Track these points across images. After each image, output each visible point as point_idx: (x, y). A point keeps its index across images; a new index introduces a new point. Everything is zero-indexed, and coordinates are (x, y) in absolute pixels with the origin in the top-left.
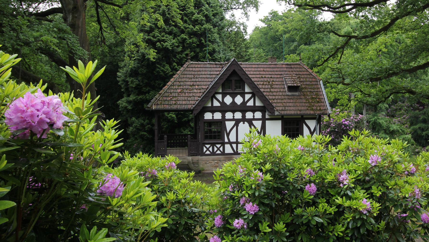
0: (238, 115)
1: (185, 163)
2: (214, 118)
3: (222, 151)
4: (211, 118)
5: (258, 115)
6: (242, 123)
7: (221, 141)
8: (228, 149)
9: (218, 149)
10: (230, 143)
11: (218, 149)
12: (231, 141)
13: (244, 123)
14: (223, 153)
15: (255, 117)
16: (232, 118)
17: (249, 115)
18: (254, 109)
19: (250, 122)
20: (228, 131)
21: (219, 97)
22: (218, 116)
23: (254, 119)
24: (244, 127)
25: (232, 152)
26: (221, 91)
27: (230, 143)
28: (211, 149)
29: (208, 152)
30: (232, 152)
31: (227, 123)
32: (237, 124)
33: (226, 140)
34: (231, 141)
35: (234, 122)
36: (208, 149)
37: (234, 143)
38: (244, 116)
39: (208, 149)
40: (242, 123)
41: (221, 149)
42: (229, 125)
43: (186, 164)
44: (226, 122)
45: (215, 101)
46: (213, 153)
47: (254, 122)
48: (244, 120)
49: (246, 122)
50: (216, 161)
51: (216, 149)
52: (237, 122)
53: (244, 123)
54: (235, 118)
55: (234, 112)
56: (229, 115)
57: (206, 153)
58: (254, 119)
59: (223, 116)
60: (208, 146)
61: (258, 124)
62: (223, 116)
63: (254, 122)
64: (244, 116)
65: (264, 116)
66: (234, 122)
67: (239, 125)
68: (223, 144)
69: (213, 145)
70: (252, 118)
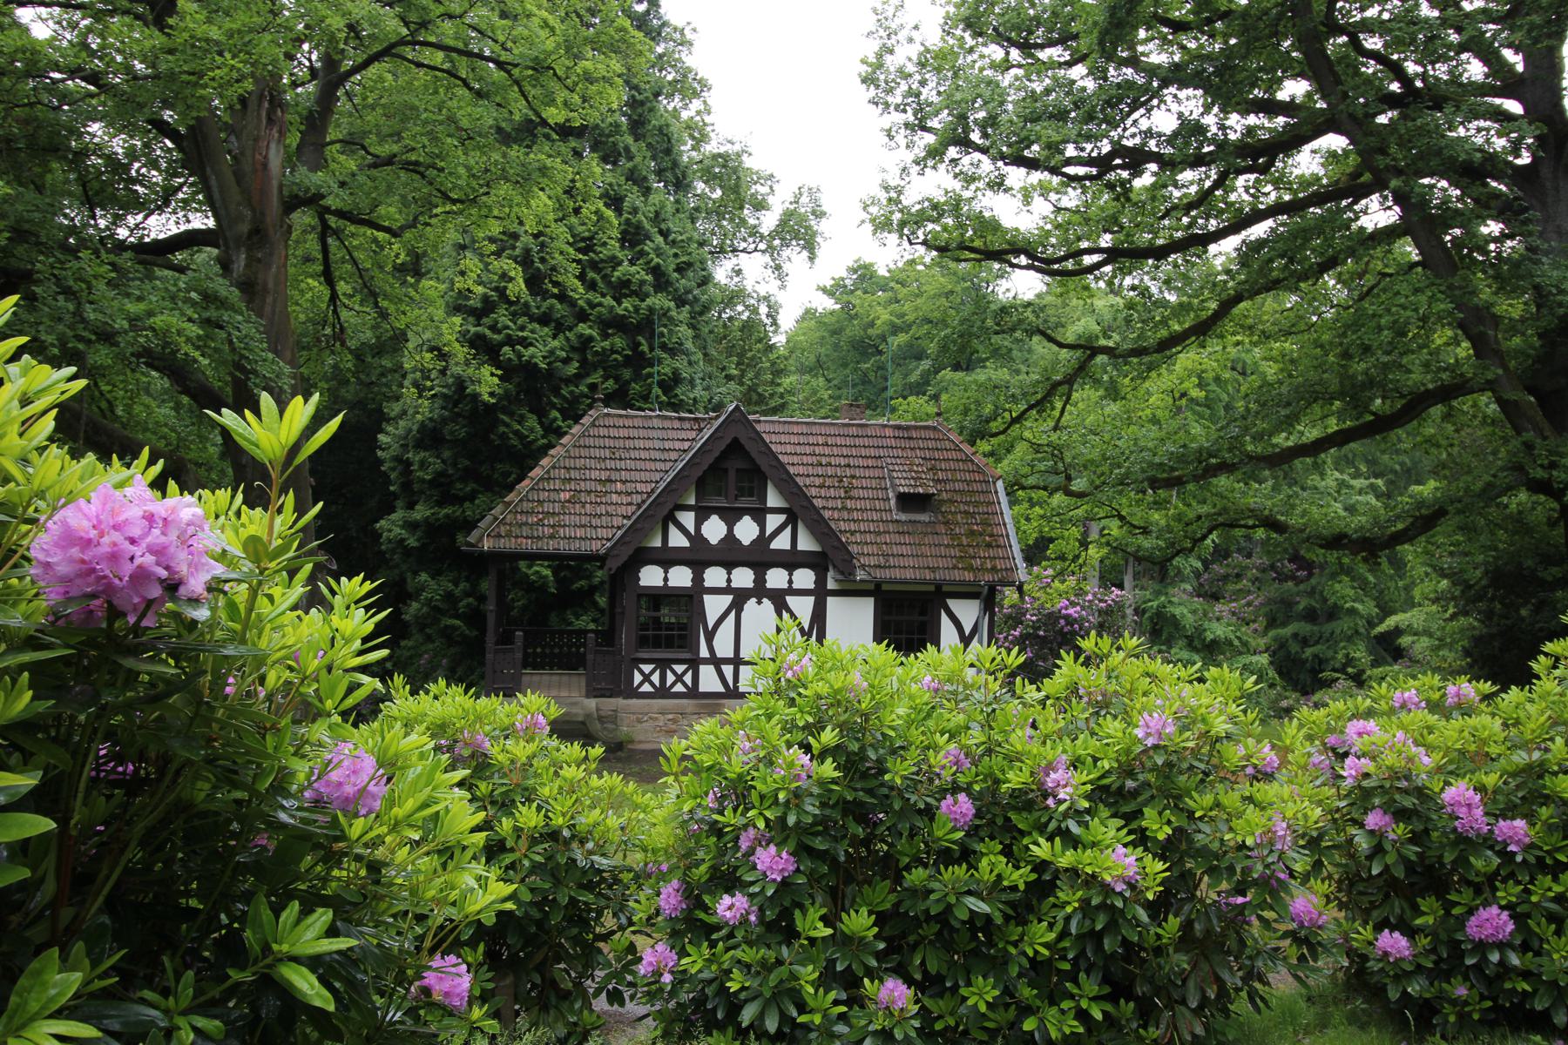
0: (743, 578)
2: (670, 584)
4: (661, 584)
5: (805, 578)
6: (754, 600)
7: (687, 656)
8: (709, 680)
9: (679, 678)
10: (717, 662)
11: (679, 678)
12: (719, 655)
13: (759, 603)
14: (693, 692)
15: (795, 586)
16: (724, 585)
17: (776, 578)
18: (791, 561)
19: (779, 600)
20: (710, 627)
21: (688, 519)
22: (681, 577)
23: (792, 591)
24: (759, 614)
25: (721, 689)
26: (692, 502)
27: (717, 662)
29: (646, 688)
30: (721, 689)
32: (737, 606)
33: (704, 652)
35: (728, 599)
36: (647, 678)
37: (727, 661)
38: (760, 580)
40: (754, 600)
41: (688, 678)
42: (714, 606)
44: (706, 598)
46: (663, 692)
47: (790, 600)
48: (759, 591)
49: (765, 600)
51: (670, 678)
52: (740, 598)
53: (759, 603)
54: (733, 585)
55: (729, 566)
56: (715, 576)
58: (792, 591)
59: (698, 579)
60: (647, 668)
61: (803, 607)
62: (698, 579)
63: (790, 600)
64: (760, 580)
65: (821, 581)
66: (727, 600)
68: (694, 663)
69: (663, 665)
70: (786, 586)
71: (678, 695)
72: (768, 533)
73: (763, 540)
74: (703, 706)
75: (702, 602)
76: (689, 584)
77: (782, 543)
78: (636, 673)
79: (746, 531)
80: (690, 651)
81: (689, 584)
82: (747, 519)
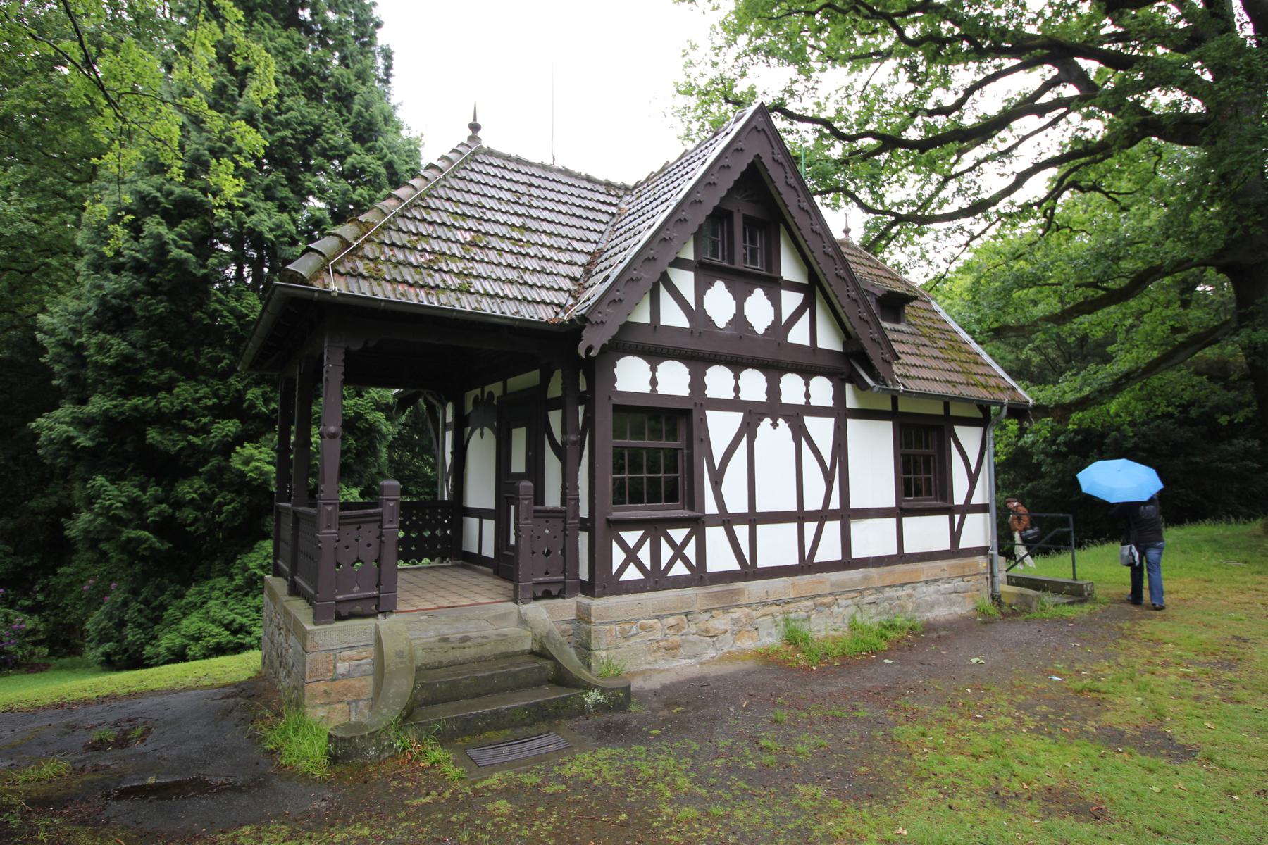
0: (754, 385)
1: (517, 648)
2: (661, 390)
3: (693, 561)
4: (647, 389)
6: (767, 421)
10: (727, 521)
12: (731, 510)
13: (775, 425)
14: (699, 576)
17: (792, 389)
19: (795, 417)
21: (685, 281)
25: (735, 566)
26: (689, 254)
27: (727, 521)
28: (645, 555)
29: (632, 573)
30: (735, 566)
31: (712, 416)
32: (748, 430)
33: (711, 507)
34: (731, 510)
35: (736, 418)
36: (631, 555)
37: (739, 518)
38: (773, 391)
39: (631, 555)
40: (767, 421)
41: (690, 551)
43: (523, 653)
44: (712, 416)
45: (665, 298)
46: (656, 579)
47: (811, 422)
48: (773, 408)
49: (781, 421)
50: (672, 621)
51: (667, 552)
52: (753, 415)
53: (775, 425)
54: (744, 396)
55: (737, 365)
56: (719, 381)
57: (624, 578)
59: (697, 384)
60: (631, 537)
62: (697, 384)
63: (811, 422)
64: (773, 391)
65: (839, 396)
66: (736, 418)
67: (759, 430)
68: (697, 525)
70: (802, 401)
71: (679, 582)
72: (785, 318)
73: (779, 328)
74: (717, 596)
75: (703, 421)
76: (685, 391)
77: (799, 335)
78: (615, 547)
79: (759, 311)
80: (692, 508)
81: (685, 391)
82: (759, 293)
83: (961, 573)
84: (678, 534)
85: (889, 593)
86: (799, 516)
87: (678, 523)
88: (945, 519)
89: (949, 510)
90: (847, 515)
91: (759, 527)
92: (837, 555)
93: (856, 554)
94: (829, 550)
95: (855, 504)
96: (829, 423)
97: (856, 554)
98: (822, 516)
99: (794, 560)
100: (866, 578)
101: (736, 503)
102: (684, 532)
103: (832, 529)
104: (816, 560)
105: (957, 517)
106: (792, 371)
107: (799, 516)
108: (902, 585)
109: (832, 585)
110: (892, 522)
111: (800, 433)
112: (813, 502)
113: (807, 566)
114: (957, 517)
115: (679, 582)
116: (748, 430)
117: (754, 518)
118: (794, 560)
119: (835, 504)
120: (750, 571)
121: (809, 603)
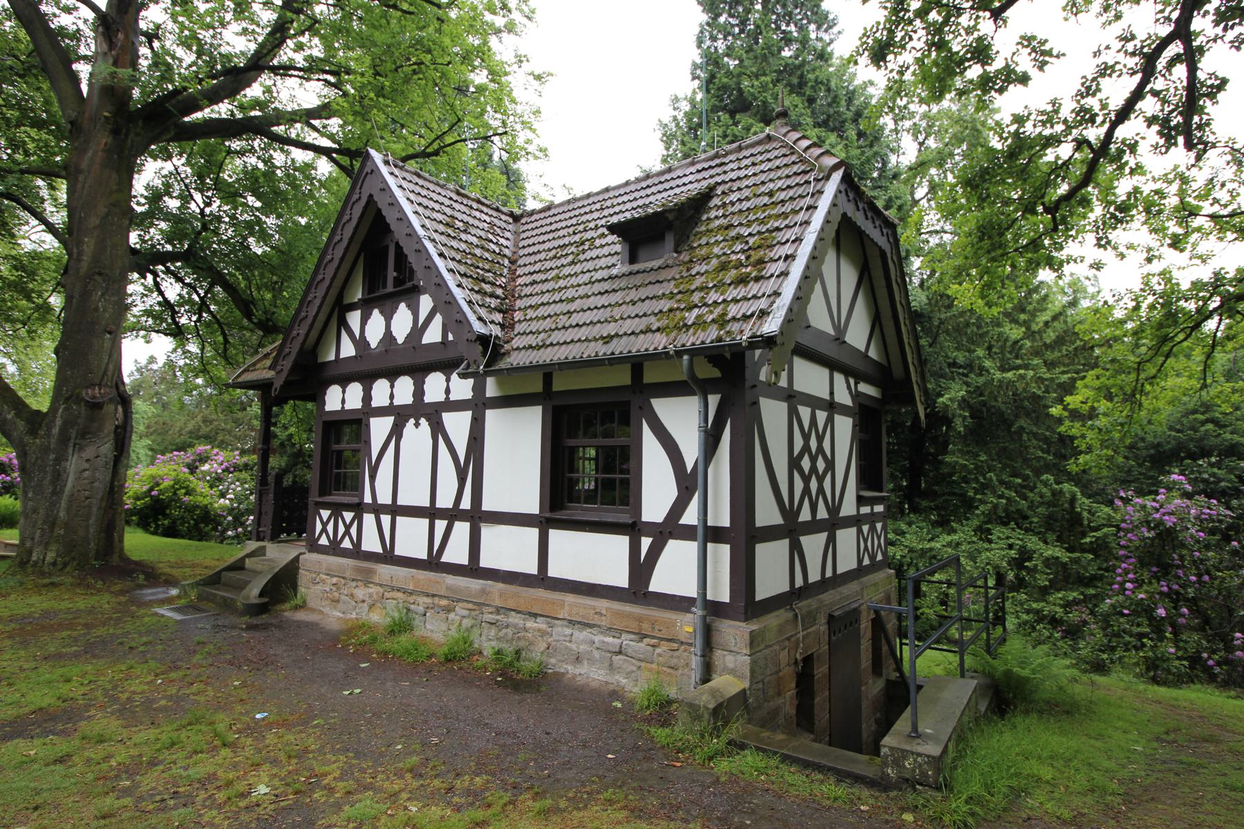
0: (404, 390)
10: (377, 509)
12: (380, 501)
13: (417, 425)
14: (357, 552)
17: (435, 386)
19: (433, 415)
27: (377, 509)
32: (397, 432)
33: (368, 499)
34: (380, 501)
35: (389, 421)
38: (419, 392)
42: (380, 428)
52: (401, 415)
53: (417, 425)
55: (392, 375)
56: (381, 392)
60: (325, 514)
64: (419, 392)
66: (389, 421)
67: (405, 431)
70: (442, 398)
75: (368, 426)
83: (633, 626)
84: (348, 516)
85: (515, 619)
86: (431, 513)
87: (349, 507)
88: (621, 543)
89: (634, 529)
90: (478, 517)
91: (399, 519)
92: (463, 559)
93: (485, 562)
94: (457, 552)
95: (487, 506)
96: (466, 417)
97: (485, 562)
98: (453, 515)
99: (423, 555)
100: (483, 591)
101: (384, 498)
102: (329, 512)
103: (462, 529)
104: (443, 560)
105: (646, 542)
106: (404, 374)
107: (431, 513)
108: (535, 615)
109: (448, 588)
110: (534, 533)
111: (438, 429)
112: (445, 500)
113: (433, 563)
114: (646, 542)
115: (345, 553)
116: (397, 432)
117: (396, 510)
118: (423, 555)
119: (466, 504)
120: (388, 556)
121: (428, 600)
